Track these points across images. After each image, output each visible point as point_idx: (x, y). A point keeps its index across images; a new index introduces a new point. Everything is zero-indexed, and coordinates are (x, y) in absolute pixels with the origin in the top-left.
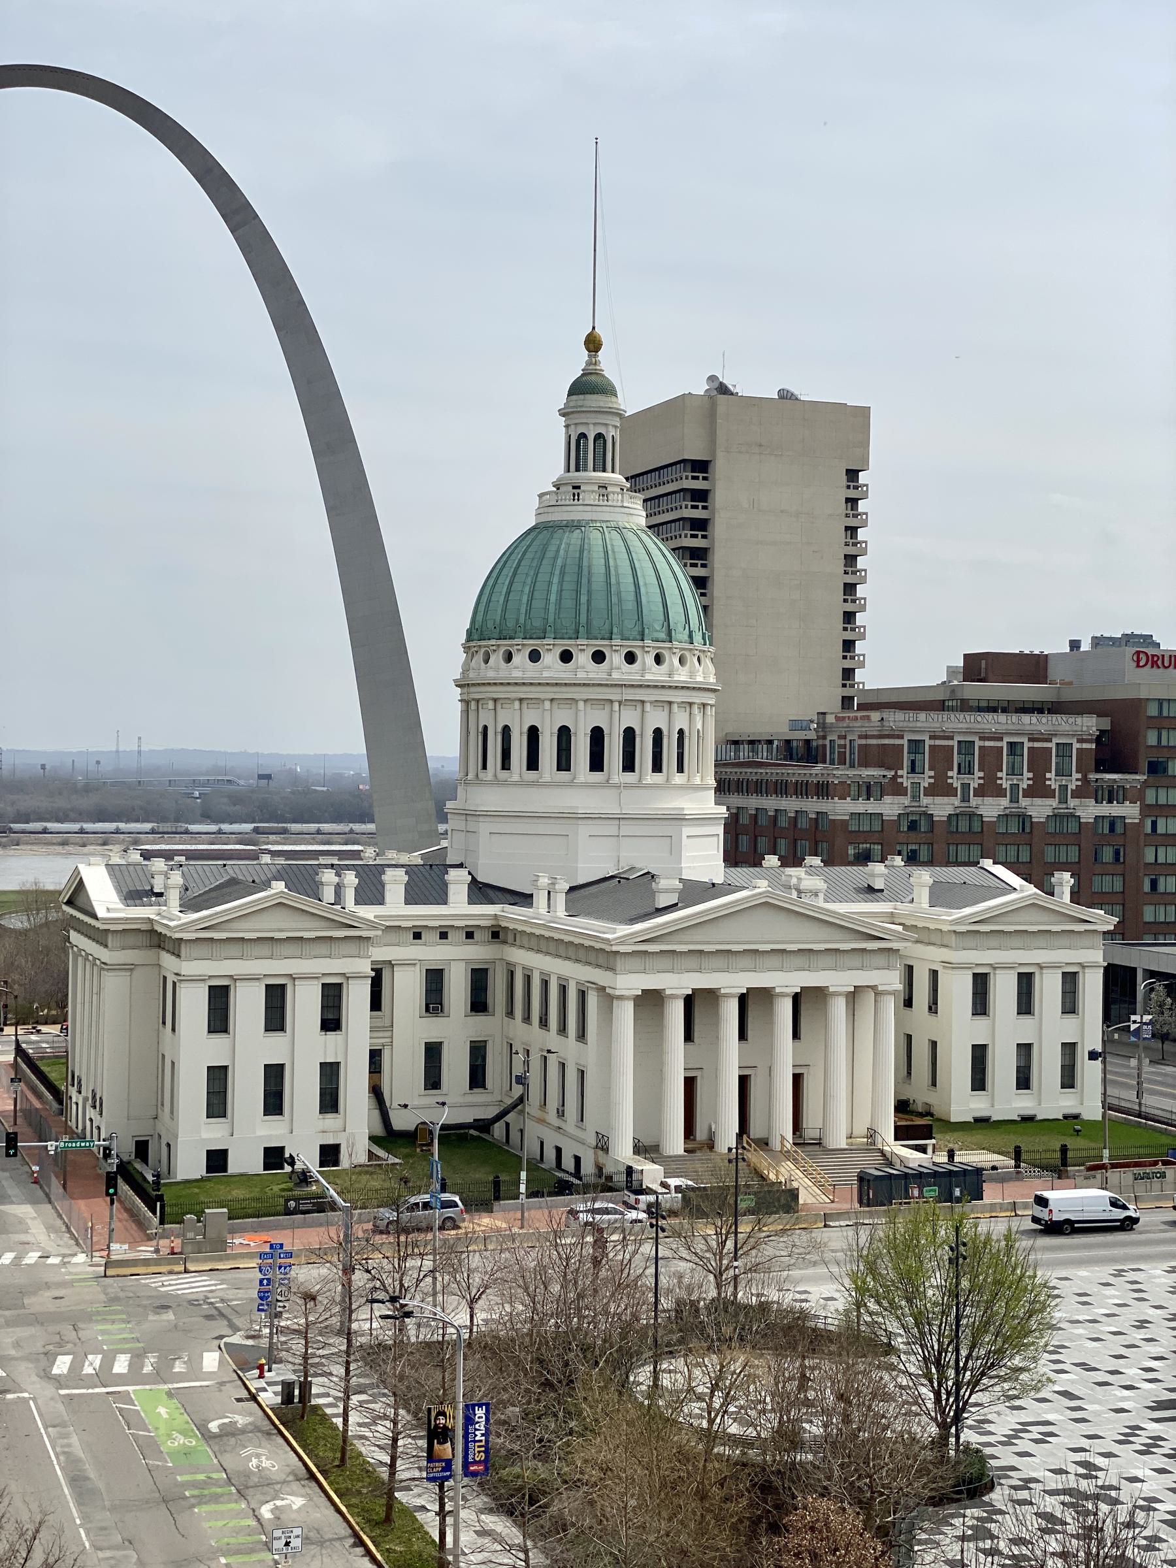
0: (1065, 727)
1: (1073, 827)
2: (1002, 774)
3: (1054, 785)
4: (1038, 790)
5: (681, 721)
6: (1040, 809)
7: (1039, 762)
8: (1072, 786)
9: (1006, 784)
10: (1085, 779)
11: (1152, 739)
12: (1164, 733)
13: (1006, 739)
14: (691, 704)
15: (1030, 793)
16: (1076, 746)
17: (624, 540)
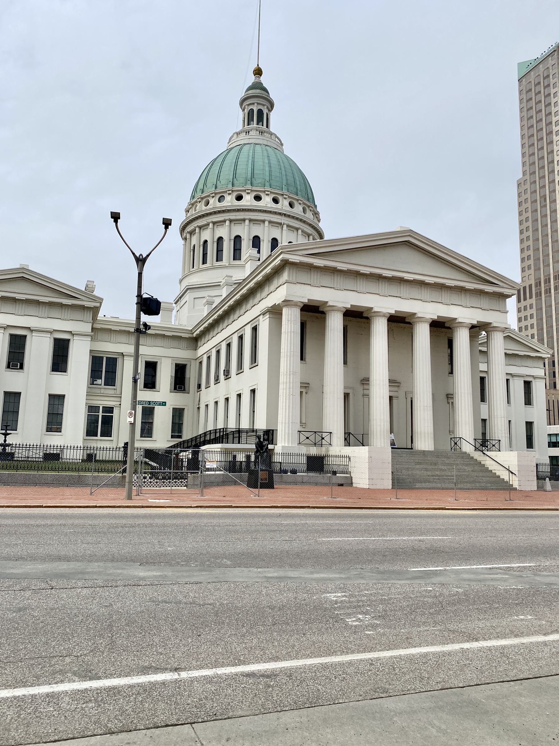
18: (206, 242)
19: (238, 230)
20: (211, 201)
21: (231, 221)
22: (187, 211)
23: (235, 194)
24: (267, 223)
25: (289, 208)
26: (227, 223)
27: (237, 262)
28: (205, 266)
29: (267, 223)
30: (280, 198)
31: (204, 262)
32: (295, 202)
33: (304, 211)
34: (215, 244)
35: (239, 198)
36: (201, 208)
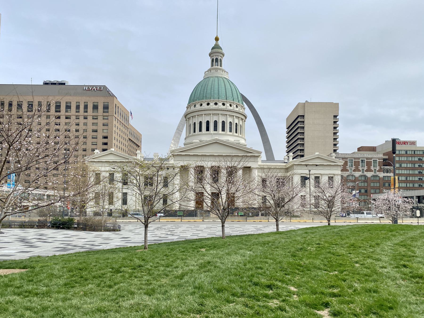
0: (375, 156)
1: (378, 179)
2: (360, 167)
3: (373, 169)
4: (369, 170)
5: (236, 121)
6: (369, 174)
7: (369, 164)
8: (377, 169)
9: (361, 169)
10: (381, 168)
11: (397, 159)
12: (401, 158)
13: (361, 159)
14: (239, 117)
15: (367, 171)
16: (378, 160)
17: (224, 81)
18: (195, 123)
19: (208, 118)
20: (197, 106)
21: (205, 114)
22: (187, 108)
23: (206, 103)
24: (220, 115)
25: (230, 108)
26: (204, 115)
27: (208, 132)
28: (194, 134)
29: (220, 115)
30: (225, 103)
31: (194, 132)
32: (232, 104)
33: (237, 106)
34: (199, 125)
35: (208, 104)
36: (193, 108)
